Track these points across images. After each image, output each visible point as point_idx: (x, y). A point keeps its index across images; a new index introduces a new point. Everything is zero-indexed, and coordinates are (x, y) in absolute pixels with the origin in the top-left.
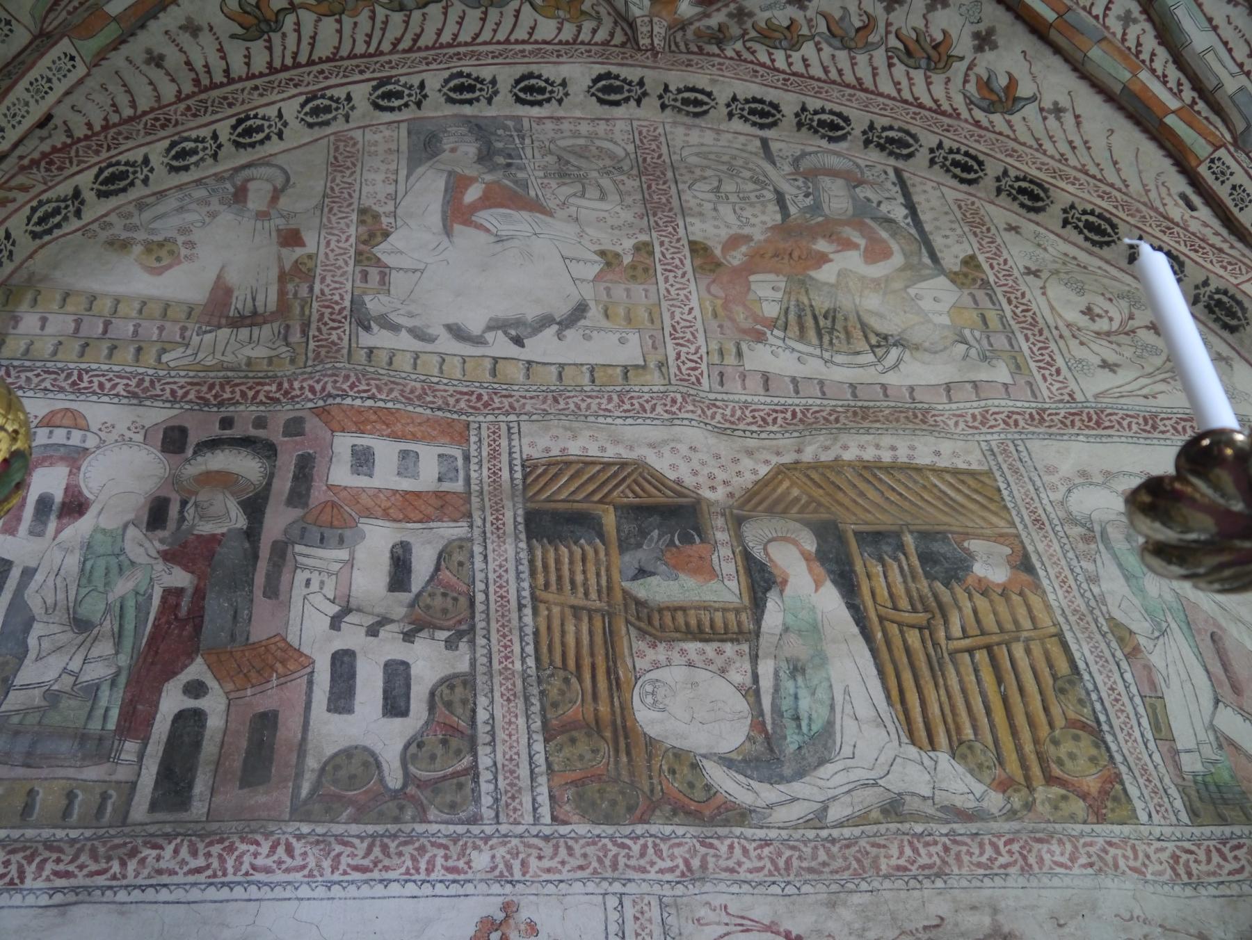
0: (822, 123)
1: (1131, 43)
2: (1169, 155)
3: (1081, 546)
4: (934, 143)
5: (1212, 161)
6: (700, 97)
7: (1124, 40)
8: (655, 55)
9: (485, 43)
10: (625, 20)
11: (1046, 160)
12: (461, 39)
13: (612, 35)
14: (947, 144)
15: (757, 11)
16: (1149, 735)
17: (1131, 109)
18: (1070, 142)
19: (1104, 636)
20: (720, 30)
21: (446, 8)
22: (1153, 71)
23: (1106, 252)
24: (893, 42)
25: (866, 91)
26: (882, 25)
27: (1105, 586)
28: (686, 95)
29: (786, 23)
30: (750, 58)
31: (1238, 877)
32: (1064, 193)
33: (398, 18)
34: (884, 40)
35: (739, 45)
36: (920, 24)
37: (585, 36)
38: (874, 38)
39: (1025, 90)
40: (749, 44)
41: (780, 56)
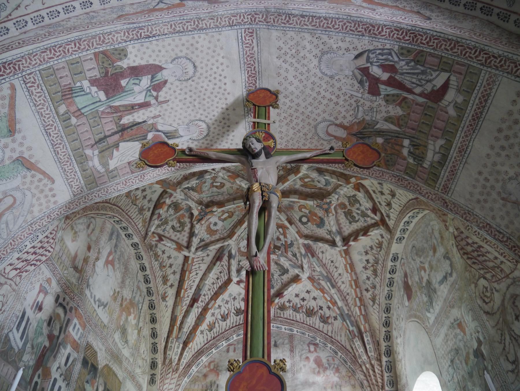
0: (147, 279)
4: (154, 299)
23: (151, 338)
24: (164, 273)
32: (157, 326)
34: (163, 272)
38: (164, 270)
39: (167, 299)
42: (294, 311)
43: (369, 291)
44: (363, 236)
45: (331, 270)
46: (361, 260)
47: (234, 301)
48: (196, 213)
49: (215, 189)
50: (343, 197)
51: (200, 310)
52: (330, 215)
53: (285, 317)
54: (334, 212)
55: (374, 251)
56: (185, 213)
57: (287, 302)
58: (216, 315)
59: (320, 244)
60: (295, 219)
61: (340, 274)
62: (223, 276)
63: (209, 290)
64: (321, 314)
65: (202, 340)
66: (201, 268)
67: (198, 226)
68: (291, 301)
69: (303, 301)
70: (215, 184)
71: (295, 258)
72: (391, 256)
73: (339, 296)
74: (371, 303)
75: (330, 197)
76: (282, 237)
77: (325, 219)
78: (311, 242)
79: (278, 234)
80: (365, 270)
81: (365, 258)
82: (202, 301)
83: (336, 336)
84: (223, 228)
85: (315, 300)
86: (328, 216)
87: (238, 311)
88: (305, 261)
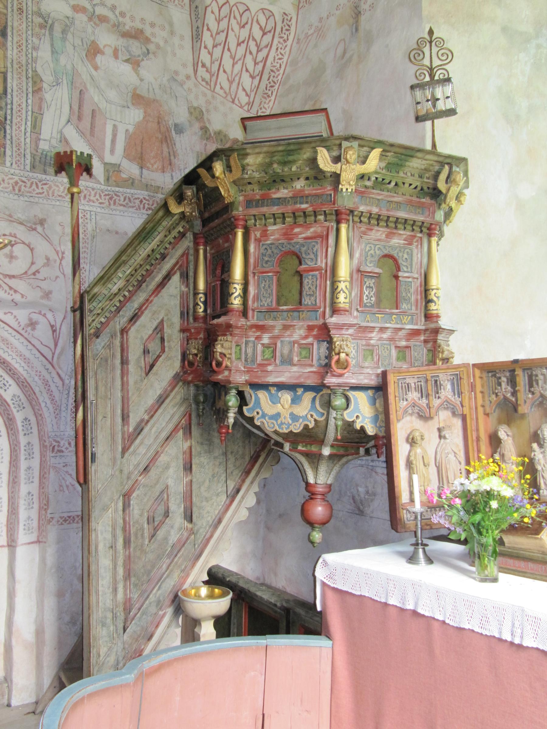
3: (37, 29)
16: (29, 130)
19: (27, 79)
27: (40, 54)
31: (39, 196)
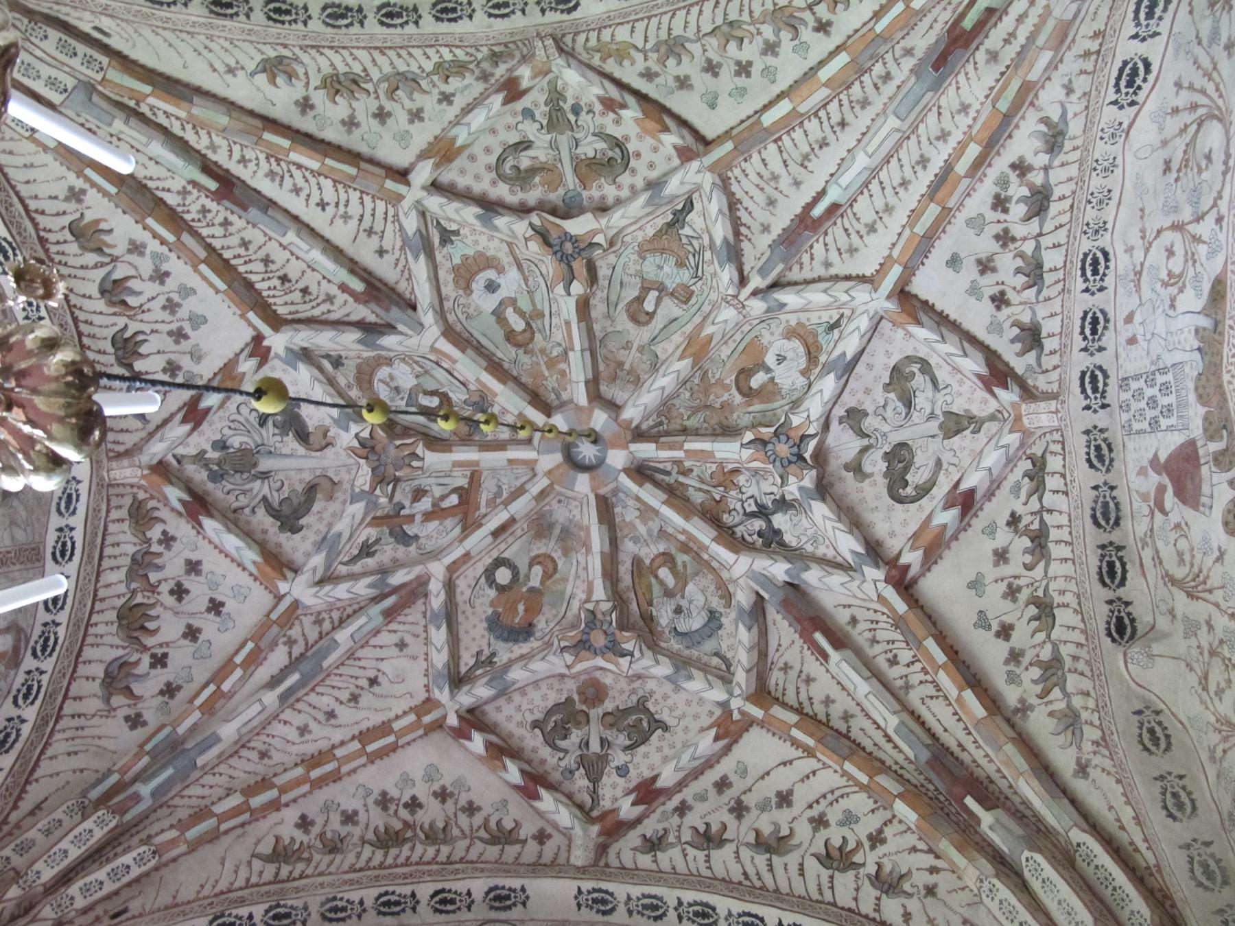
0: (399, 15)
1: (203, 133)
2: (134, 62)
5: (102, 69)
6: (496, 12)
7: (209, 133)
8: (538, 34)
9: (666, 13)
10: (567, 53)
11: (222, 34)
12: (684, 12)
13: (574, 41)
14: (300, 26)
15: (474, 83)
17: (179, 87)
18: (210, 51)
20: (497, 63)
21: (699, 31)
22: (177, 118)
24: (369, 86)
25: (376, 48)
26: (382, 96)
28: (507, 11)
29: (450, 80)
30: (468, 50)
33: (733, 16)
35: (480, 56)
36: (355, 104)
37: (593, 35)
38: (385, 85)
39: (262, 79)
40: (472, 58)
41: (448, 56)
42: (134, 559)
43: (307, 832)
44: (522, 771)
45: (333, 680)
46: (407, 780)
47: (170, 333)
48: (577, 226)
49: (632, 293)
50: (634, 691)
51: (172, 200)
52: (569, 658)
53: (112, 528)
54: (579, 667)
55: (463, 820)
56: (561, 191)
57: (164, 533)
58: (134, 258)
59: (439, 636)
60: (503, 546)
61: (331, 715)
62: (289, 298)
63: (245, 244)
64: (137, 663)
65: (43, 190)
66: (339, 222)
67: (521, 227)
68: (168, 547)
69: (172, 592)
70: (653, 295)
71: (356, 552)
72: (516, 883)
73: (255, 723)
74: (266, 848)
75: (648, 653)
76: (425, 504)
77: (534, 644)
78: (437, 601)
79: (438, 492)
80: (377, 803)
81: (422, 792)
82: (204, 211)
83: (68, 734)
84: (471, 311)
85: (185, 636)
86: (563, 649)
87: (131, 345)
88: (362, 588)
